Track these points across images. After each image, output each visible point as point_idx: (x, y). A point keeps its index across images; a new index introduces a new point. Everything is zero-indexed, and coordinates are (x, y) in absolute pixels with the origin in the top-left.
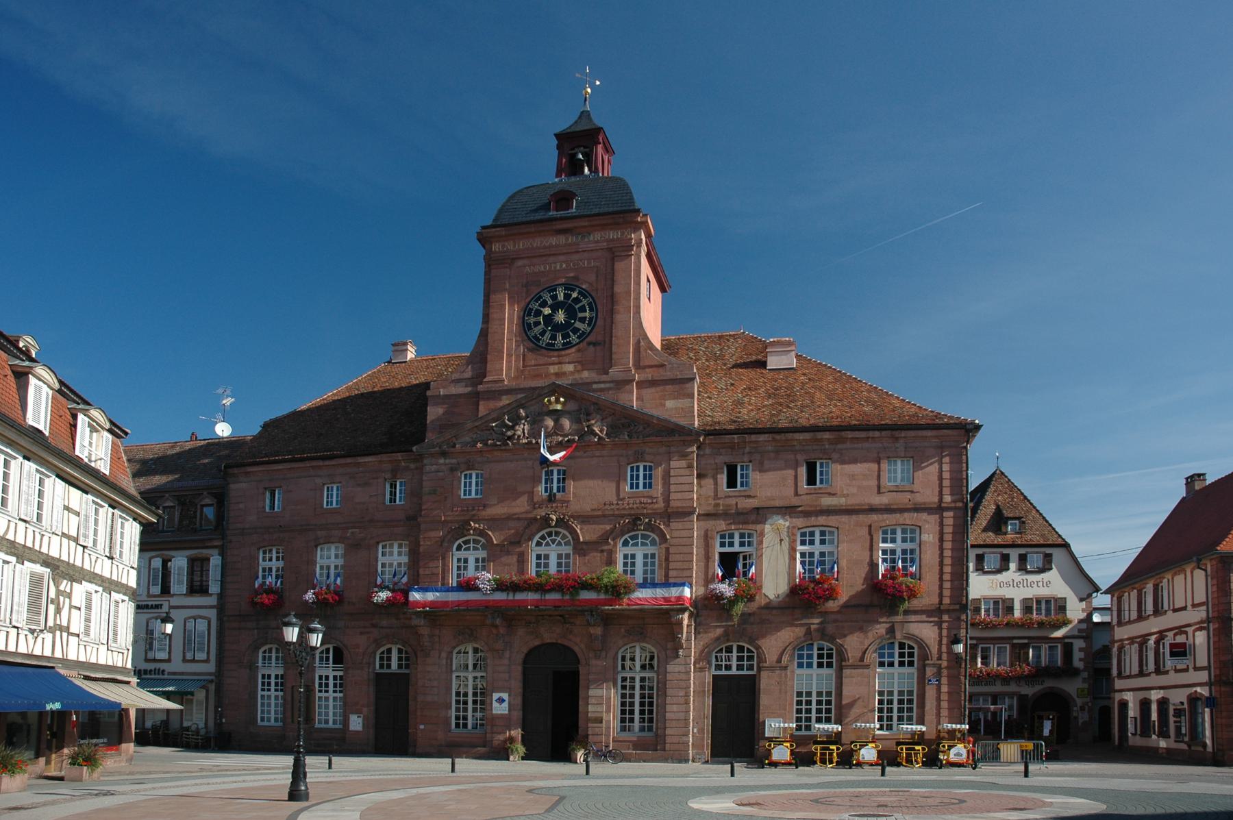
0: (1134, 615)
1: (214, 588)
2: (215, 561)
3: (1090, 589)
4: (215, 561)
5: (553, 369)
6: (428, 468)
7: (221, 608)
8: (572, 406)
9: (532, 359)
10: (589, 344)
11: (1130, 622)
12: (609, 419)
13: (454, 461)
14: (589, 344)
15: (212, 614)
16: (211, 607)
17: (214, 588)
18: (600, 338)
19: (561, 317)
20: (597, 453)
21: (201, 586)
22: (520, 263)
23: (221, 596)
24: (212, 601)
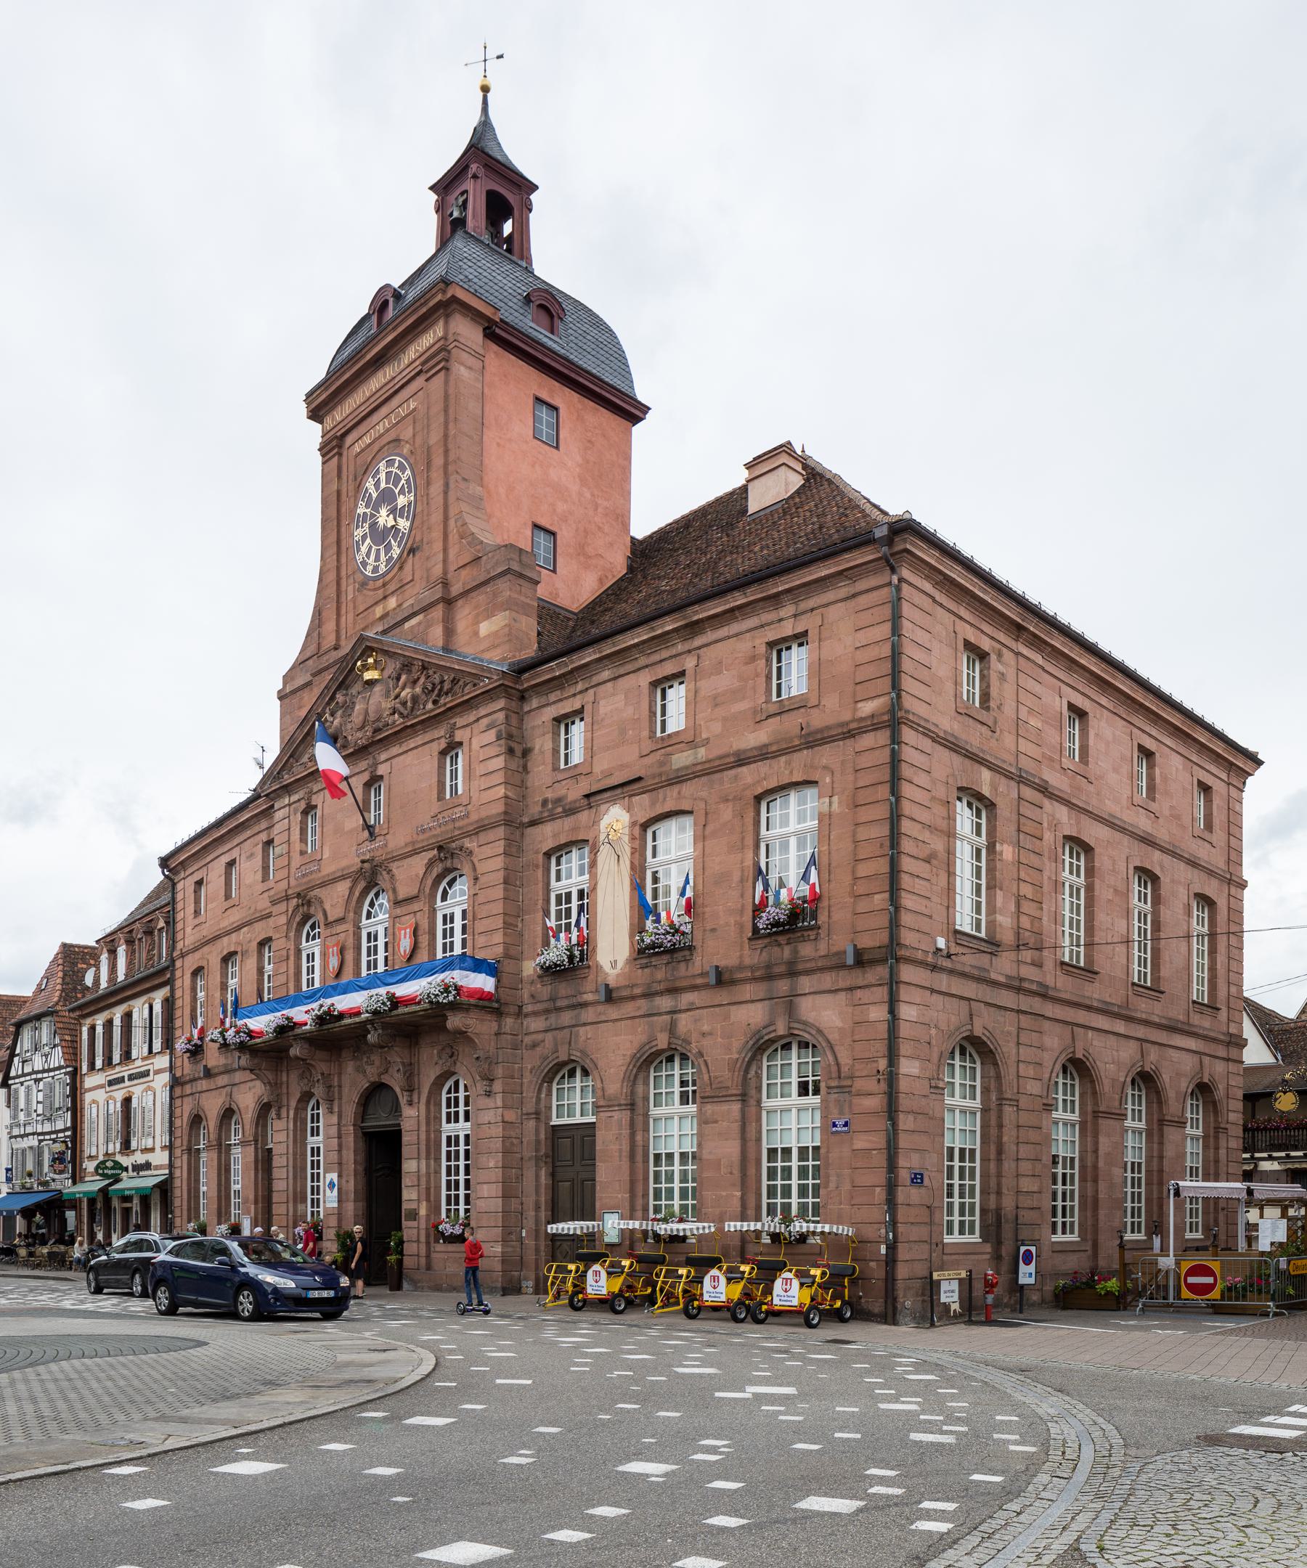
5: (379, 611)
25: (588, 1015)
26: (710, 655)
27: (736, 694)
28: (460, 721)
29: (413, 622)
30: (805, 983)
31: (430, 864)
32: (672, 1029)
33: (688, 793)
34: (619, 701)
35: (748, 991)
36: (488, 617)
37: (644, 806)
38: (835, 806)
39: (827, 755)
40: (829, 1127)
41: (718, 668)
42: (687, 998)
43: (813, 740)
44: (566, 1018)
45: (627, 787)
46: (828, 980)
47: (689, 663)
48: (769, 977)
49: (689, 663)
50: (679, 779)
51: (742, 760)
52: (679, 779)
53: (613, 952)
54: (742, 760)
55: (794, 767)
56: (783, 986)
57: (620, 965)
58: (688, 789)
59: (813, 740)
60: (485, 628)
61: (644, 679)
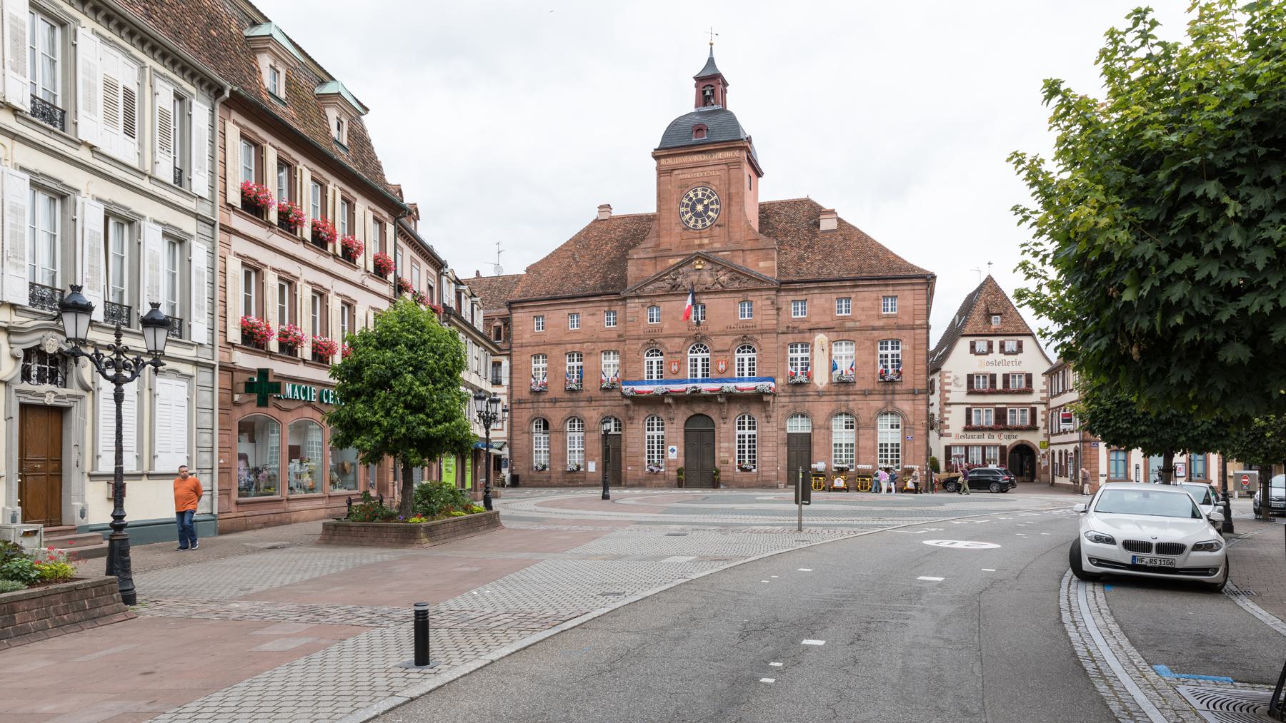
1: (505, 381)
2: (505, 363)
5: (697, 242)
7: (511, 395)
8: (708, 266)
9: (686, 234)
17: (505, 381)
19: (700, 208)
23: (511, 386)
25: (810, 399)
26: (861, 295)
27: (871, 309)
30: (897, 397)
31: (736, 340)
32: (847, 406)
33: (852, 335)
34: (823, 301)
35: (876, 397)
37: (833, 335)
39: (904, 333)
40: (904, 438)
41: (864, 299)
42: (852, 397)
43: (900, 328)
44: (799, 399)
45: (826, 329)
46: (905, 397)
47: (853, 296)
48: (885, 394)
49: (853, 296)
50: (849, 330)
51: (874, 329)
52: (849, 330)
53: (821, 378)
54: (874, 329)
55: (895, 334)
56: (889, 397)
58: (852, 334)
59: (900, 328)
60: (762, 264)
61: (834, 296)
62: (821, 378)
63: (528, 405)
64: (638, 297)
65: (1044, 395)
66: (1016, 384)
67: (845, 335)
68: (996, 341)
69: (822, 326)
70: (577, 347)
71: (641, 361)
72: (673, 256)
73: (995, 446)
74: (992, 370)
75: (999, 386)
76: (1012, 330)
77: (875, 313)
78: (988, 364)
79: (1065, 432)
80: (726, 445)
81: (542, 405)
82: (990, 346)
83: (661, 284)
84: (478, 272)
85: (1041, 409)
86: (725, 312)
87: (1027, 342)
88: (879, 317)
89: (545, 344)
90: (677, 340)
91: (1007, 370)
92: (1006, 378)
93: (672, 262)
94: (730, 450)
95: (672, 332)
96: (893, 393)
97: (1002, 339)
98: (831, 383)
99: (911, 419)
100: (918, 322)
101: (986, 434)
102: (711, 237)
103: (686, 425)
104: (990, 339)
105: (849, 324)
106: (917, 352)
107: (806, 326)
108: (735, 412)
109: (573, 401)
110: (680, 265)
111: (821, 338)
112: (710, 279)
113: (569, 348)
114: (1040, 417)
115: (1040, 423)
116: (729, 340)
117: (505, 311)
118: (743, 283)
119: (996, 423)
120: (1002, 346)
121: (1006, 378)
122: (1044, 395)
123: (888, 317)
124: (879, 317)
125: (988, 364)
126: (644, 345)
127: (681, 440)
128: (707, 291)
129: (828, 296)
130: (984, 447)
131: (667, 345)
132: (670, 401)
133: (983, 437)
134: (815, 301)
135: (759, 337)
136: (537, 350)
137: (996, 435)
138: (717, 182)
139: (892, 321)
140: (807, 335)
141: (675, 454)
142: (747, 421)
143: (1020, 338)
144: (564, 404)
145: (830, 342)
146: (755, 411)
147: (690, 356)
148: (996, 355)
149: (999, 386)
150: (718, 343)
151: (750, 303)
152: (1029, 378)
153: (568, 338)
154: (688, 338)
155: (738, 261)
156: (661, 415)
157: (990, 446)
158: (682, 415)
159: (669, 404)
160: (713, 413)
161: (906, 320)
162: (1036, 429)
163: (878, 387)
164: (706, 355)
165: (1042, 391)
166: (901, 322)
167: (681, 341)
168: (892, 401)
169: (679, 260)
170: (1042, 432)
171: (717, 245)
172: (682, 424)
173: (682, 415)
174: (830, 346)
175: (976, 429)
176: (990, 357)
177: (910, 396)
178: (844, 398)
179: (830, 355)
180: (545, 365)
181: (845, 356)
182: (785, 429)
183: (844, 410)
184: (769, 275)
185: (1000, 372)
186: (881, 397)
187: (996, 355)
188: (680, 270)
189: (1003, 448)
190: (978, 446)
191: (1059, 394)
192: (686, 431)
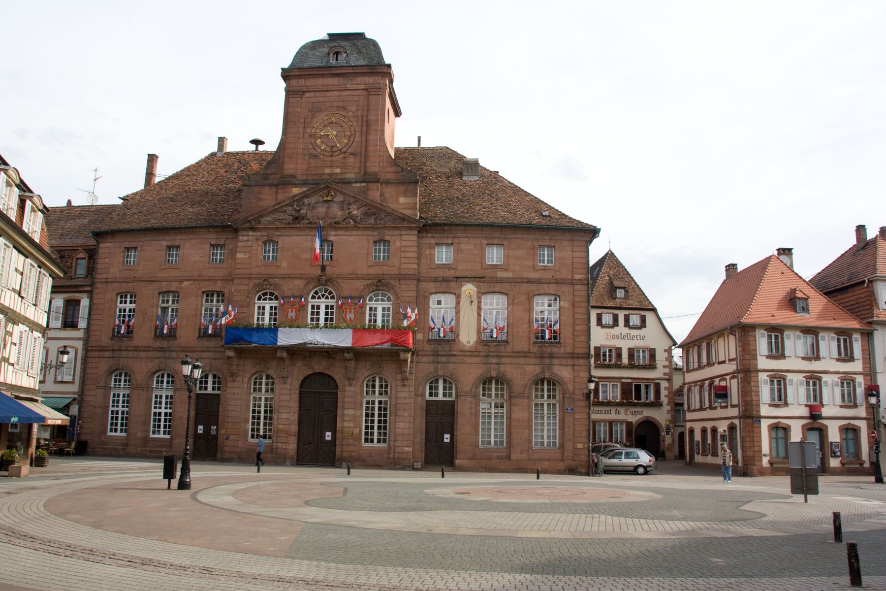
0: (696, 365)
1: (82, 324)
2: (85, 302)
3: (671, 343)
4: (85, 302)
6: (241, 238)
7: (86, 340)
10: (351, 154)
11: (694, 370)
12: (363, 209)
13: (259, 234)
14: (351, 154)
15: (79, 345)
16: (79, 339)
17: (82, 324)
18: (358, 151)
20: (354, 233)
21: (72, 322)
22: (307, 95)
23: (88, 330)
24: (80, 334)
28: (387, 232)
29: (358, 185)
30: (555, 361)
31: (369, 285)
35: (532, 361)
36: (405, 196)
38: (566, 305)
43: (558, 282)
46: (564, 361)
47: (506, 243)
48: (542, 357)
50: (501, 281)
51: (529, 281)
53: (468, 337)
55: (553, 288)
56: (547, 361)
57: (472, 343)
58: (504, 285)
60: (402, 200)
62: (468, 337)
63: (107, 354)
64: (253, 229)
65: (667, 370)
66: (641, 359)
67: (498, 287)
68: (621, 315)
69: (468, 274)
70: (174, 286)
71: (250, 305)
72: (295, 185)
73: (621, 422)
74: (618, 343)
75: (625, 360)
76: (636, 304)
77: (530, 263)
78: (615, 337)
79: (711, 408)
80: (351, 412)
81: (125, 354)
82: (616, 319)
83: (282, 216)
84: (69, 202)
85: (664, 384)
86: (355, 250)
87: (649, 316)
88: (534, 268)
89: (135, 280)
90: (296, 282)
91: (632, 344)
92: (631, 353)
93: (296, 191)
94: (356, 419)
95: (290, 272)
96: (551, 356)
97: (627, 312)
98: (481, 342)
99: (570, 387)
100: (577, 277)
101: (613, 410)
102: (343, 166)
103: (302, 386)
104: (616, 312)
105: (501, 274)
106: (577, 310)
107: (452, 273)
108: (364, 372)
109: (162, 350)
110: (305, 195)
111: (469, 289)
112: (340, 213)
113: (164, 287)
114: (664, 393)
115: (664, 399)
116: (359, 284)
117: (92, 241)
118: (379, 221)
119: (622, 398)
120: (627, 319)
121: (631, 353)
122: (667, 370)
123: (545, 269)
124: (534, 268)
125: (615, 337)
126: (256, 286)
127: (295, 405)
128: (336, 225)
129: (478, 241)
130: (611, 423)
131: (285, 289)
132: (285, 355)
133: (610, 412)
134: (463, 247)
135: (396, 283)
136: (125, 287)
137: (622, 410)
138: (354, 108)
139: (548, 275)
140: (453, 284)
141: (288, 417)
142: (377, 383)
143: (643, 313)
144: (151, 354)
145: (480, 294)
146: (389, 371)
147: (312, 302)
148: (621, 329)
149: (625, 360)
150: (348, 288)
151: (386, 242)
152: (652, 353)
153: (164, 275)
154: (309, 280)
155: (374, 194)
156: (271, 372)
157: (616, 421)
158: (299, 371)
159: (282, 359)
160: (337, 374)
161: (565, 274)
162: (661, 405)
163: (534, 349)
164: (331, 302)
165: (664, 367)
166: (558, 276)
167: (300, 283)
168: (550, 365)
169: (305, 189)
170: (666, 407)
171: (351, 176)
172: (297, 384)
173: (299, 371)
174: (479, 299)
175: (602, 404)
176: (616, 331)
177: (570, 361)
178: (494, 360)
179: (479, 308)
180: (133, 306)
181: (496, 308)
182: (423, 395)
183: (494, 374)
184: (409, 213)
185: (625, 346)
186: (537, 361)
187: (621, 329)
188: (306, 201)
189: (629, 424)
190: (604, 421)
191: (700, 367)
192: (301, 394)
